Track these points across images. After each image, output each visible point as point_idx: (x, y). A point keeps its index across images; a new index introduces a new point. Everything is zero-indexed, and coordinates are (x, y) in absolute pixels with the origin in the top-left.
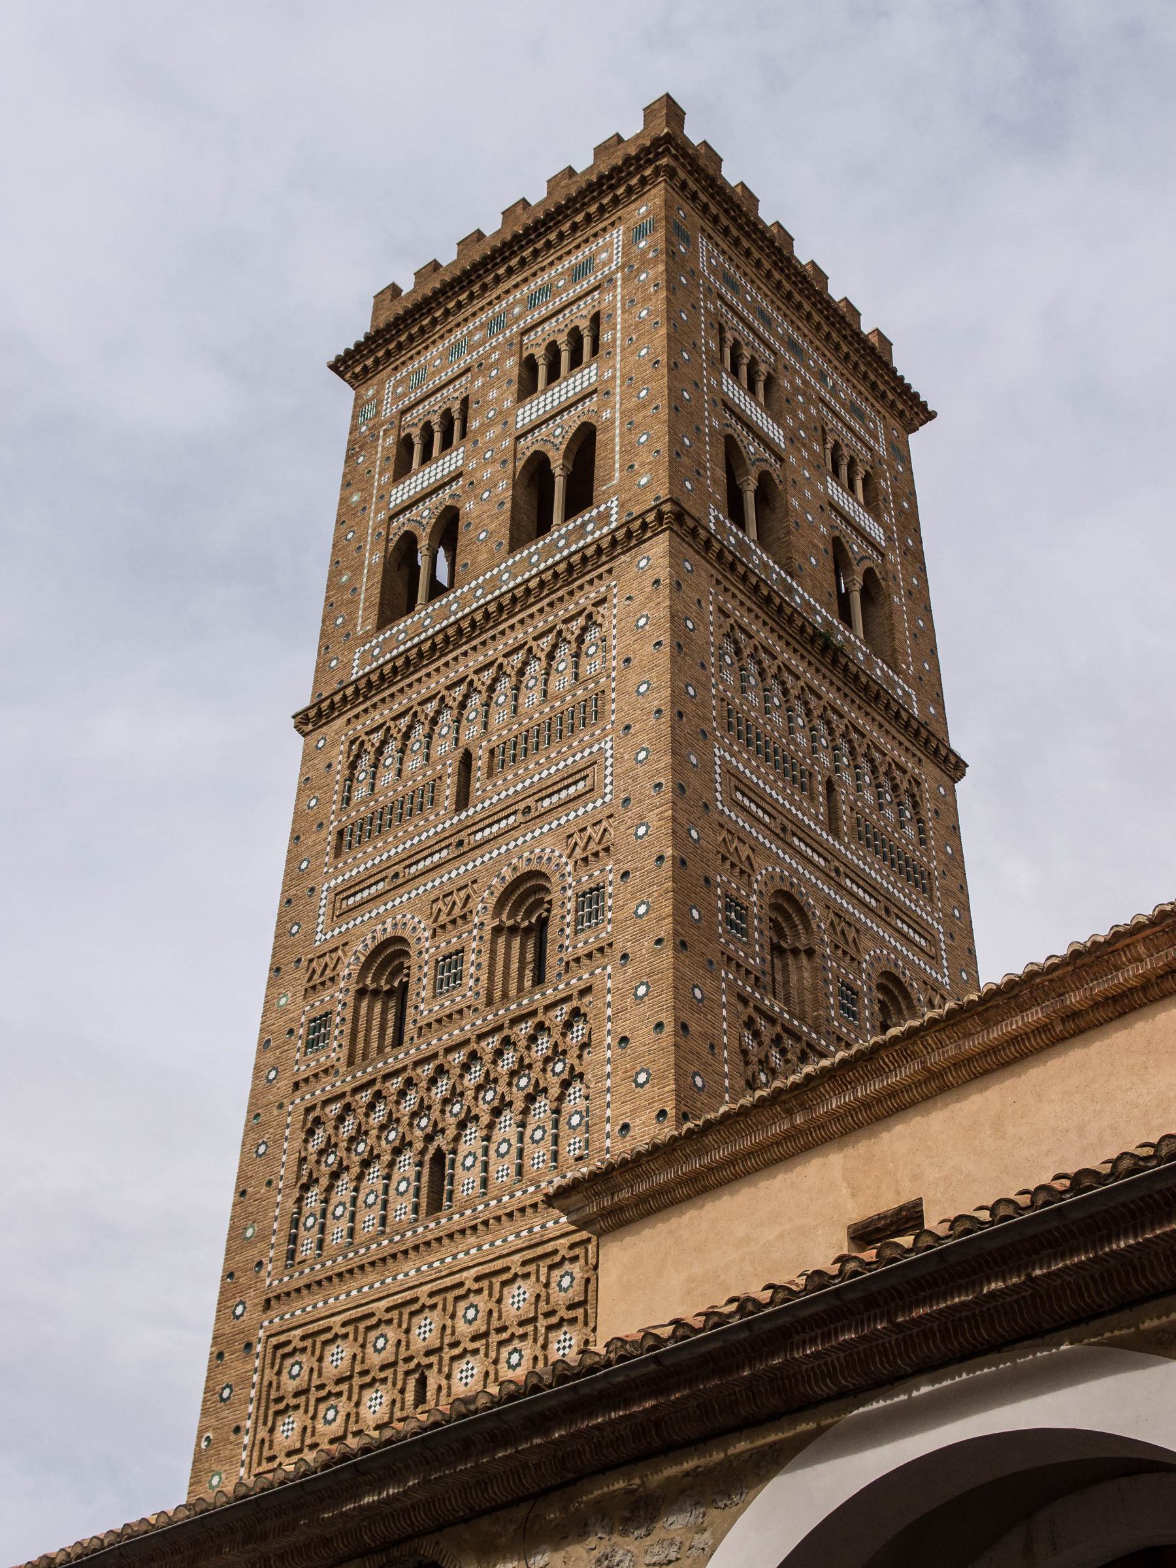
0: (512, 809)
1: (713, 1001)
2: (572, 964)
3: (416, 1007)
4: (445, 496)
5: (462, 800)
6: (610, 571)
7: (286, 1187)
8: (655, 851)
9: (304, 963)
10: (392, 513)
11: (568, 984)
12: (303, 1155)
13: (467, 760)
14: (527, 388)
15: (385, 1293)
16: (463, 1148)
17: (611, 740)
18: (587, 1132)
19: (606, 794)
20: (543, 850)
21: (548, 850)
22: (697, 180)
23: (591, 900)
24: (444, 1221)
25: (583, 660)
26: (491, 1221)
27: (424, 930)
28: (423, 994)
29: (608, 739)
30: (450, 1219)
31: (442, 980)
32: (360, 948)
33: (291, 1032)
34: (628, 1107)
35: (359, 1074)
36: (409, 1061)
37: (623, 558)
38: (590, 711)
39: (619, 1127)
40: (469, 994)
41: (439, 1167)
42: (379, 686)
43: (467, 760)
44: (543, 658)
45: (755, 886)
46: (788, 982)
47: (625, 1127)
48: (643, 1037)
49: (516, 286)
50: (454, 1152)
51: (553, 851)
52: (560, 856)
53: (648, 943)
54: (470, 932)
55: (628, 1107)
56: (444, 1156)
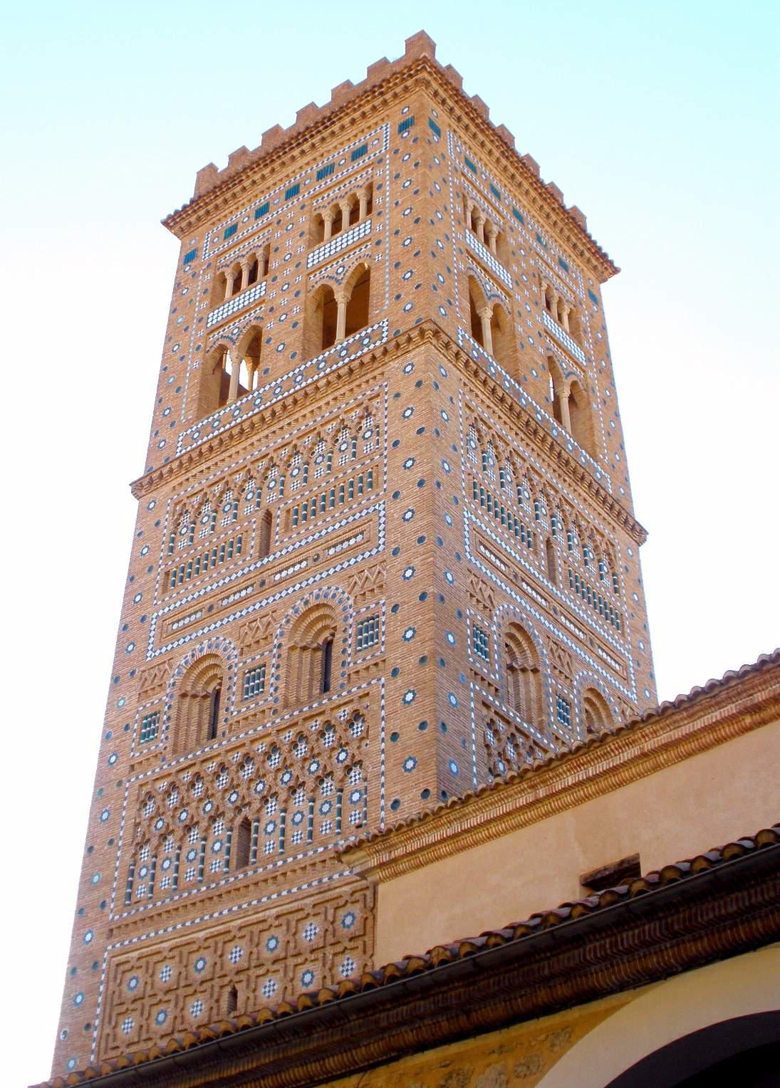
0: (304, 556)
2: (353, 676)
3: (227, 710)
5: (265, 550)
6: (382, 374)
7: (124, 845)
11: (349, 692)
12: (138, 821)
13: (268, 517)
14: (317, 237)
15: (204, 927)
17: (384, 503)
18: (366, 806)
19: (380, 545)
20: (329, 588)
21: (333, 588)
22: (446, 90)
23: (369, 628)
24: (250, 873)
26: (289, 873)
27: (234, 649)
28: (233, 698)
29: (381, 502)
30: (255, 872)
31: (248, 688)
33: (127, 727)
34: (398, 788)
35: (182, 760)
36: (222, 750)
39: (391, 803)
40: (270, 698)
43: (268, 517)
44: (329, 440)
45: (495, 619)
46: (519, 694)
47: (396, 803)
48: (410, 733)
50: (258, 821)
51: (337, 589)
52: (343, 593)
53: (414, 659)
54: (271, 651)
55: (398, 788)
56: (250, 824)
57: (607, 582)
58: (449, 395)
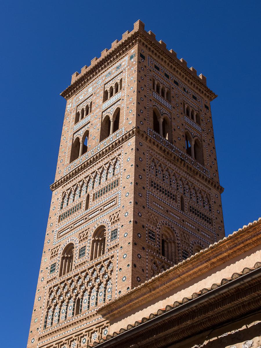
0: (98, 209)
1: (144, 258)
2: (110, 249)
3: (75, 261)
4: (86, 128)
5: (87, 208)
6: (122, 147)
7: (45, 308)
8: (129, 220)
9: (51, 250)
10: (74, 132)
11: (109, 255)
12: (48, 300)
13: (88, 196)
14: (105, 99)
15: (65, 336)
16: (84, 298)
17: (120, 191)
20: (104, 220)
21: (105, 220)
22: (147, 42)
23: (114, 234)
24: (79, 317)
25: (116, 170)
26: (89, 317)
27: (77, 241)
28: (76, 258)
29: (120, 190)
30: (80, 316)
31: (81, 254)
32: (63, 246)
33: (47, 268)
34: (120, 287)
36: (73, 275)
37: (125, 143)
38: (116, 183)
39: (119, 292)
40: (87, 257)
41: (78, 303)
42: (69, 178)
43: (88, 196)
44: (106, 170)
45: (158, 227)
46: (168, 251)
47: (120, 292)
49: (104, 72)
50: (82, 299)
51: (106, 220)
52: (108, 221)
53: (127, 244)
54: (87, 241)
57: (207, 207)
58: (143, 152)
